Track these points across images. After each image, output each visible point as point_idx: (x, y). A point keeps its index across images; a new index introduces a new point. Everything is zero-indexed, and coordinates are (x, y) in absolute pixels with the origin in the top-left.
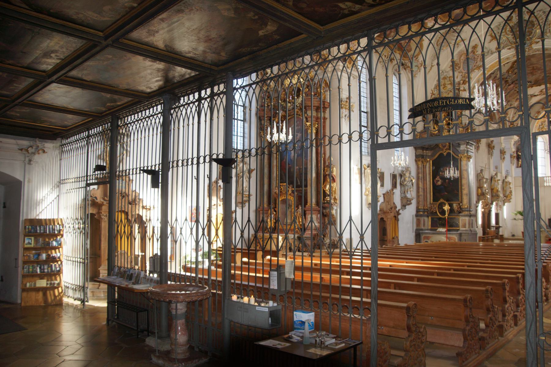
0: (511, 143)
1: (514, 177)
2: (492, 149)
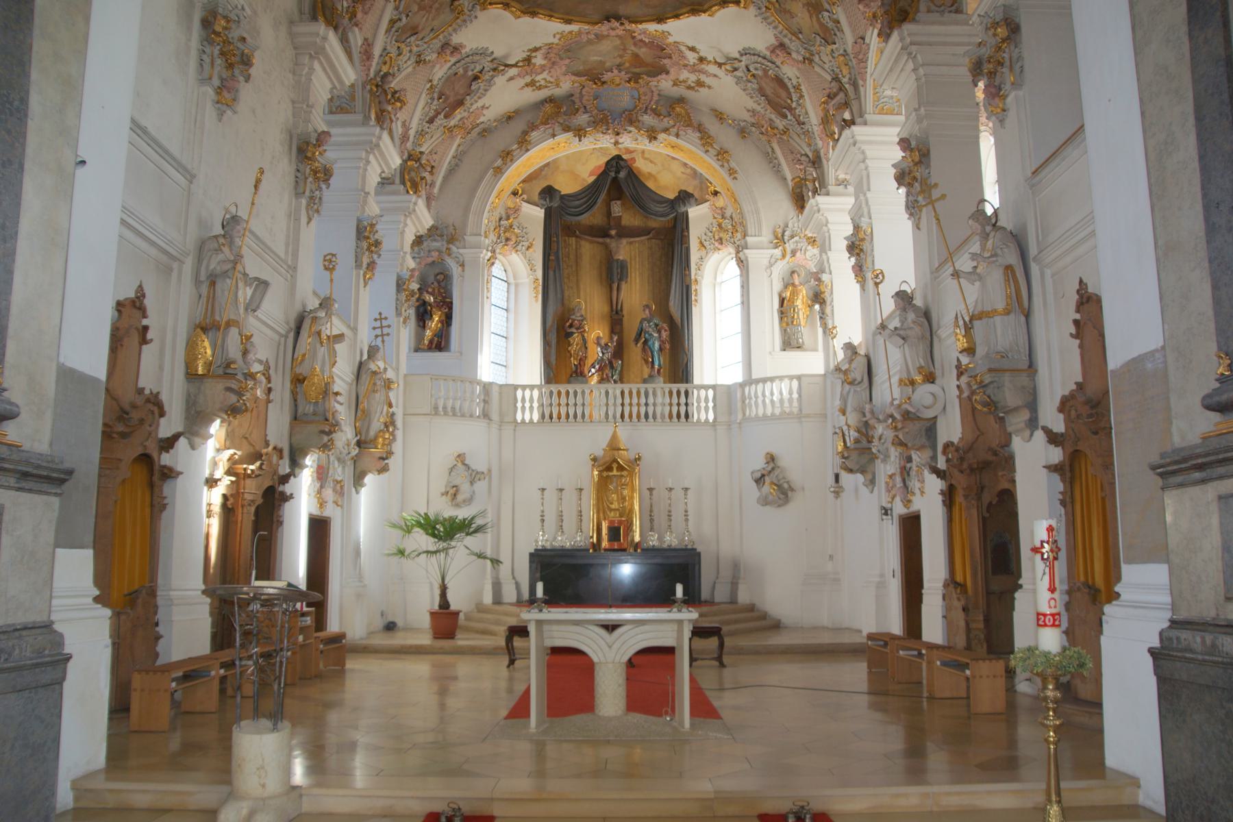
0: (403, 233)
1: (405, 376)
2: (315, 172)
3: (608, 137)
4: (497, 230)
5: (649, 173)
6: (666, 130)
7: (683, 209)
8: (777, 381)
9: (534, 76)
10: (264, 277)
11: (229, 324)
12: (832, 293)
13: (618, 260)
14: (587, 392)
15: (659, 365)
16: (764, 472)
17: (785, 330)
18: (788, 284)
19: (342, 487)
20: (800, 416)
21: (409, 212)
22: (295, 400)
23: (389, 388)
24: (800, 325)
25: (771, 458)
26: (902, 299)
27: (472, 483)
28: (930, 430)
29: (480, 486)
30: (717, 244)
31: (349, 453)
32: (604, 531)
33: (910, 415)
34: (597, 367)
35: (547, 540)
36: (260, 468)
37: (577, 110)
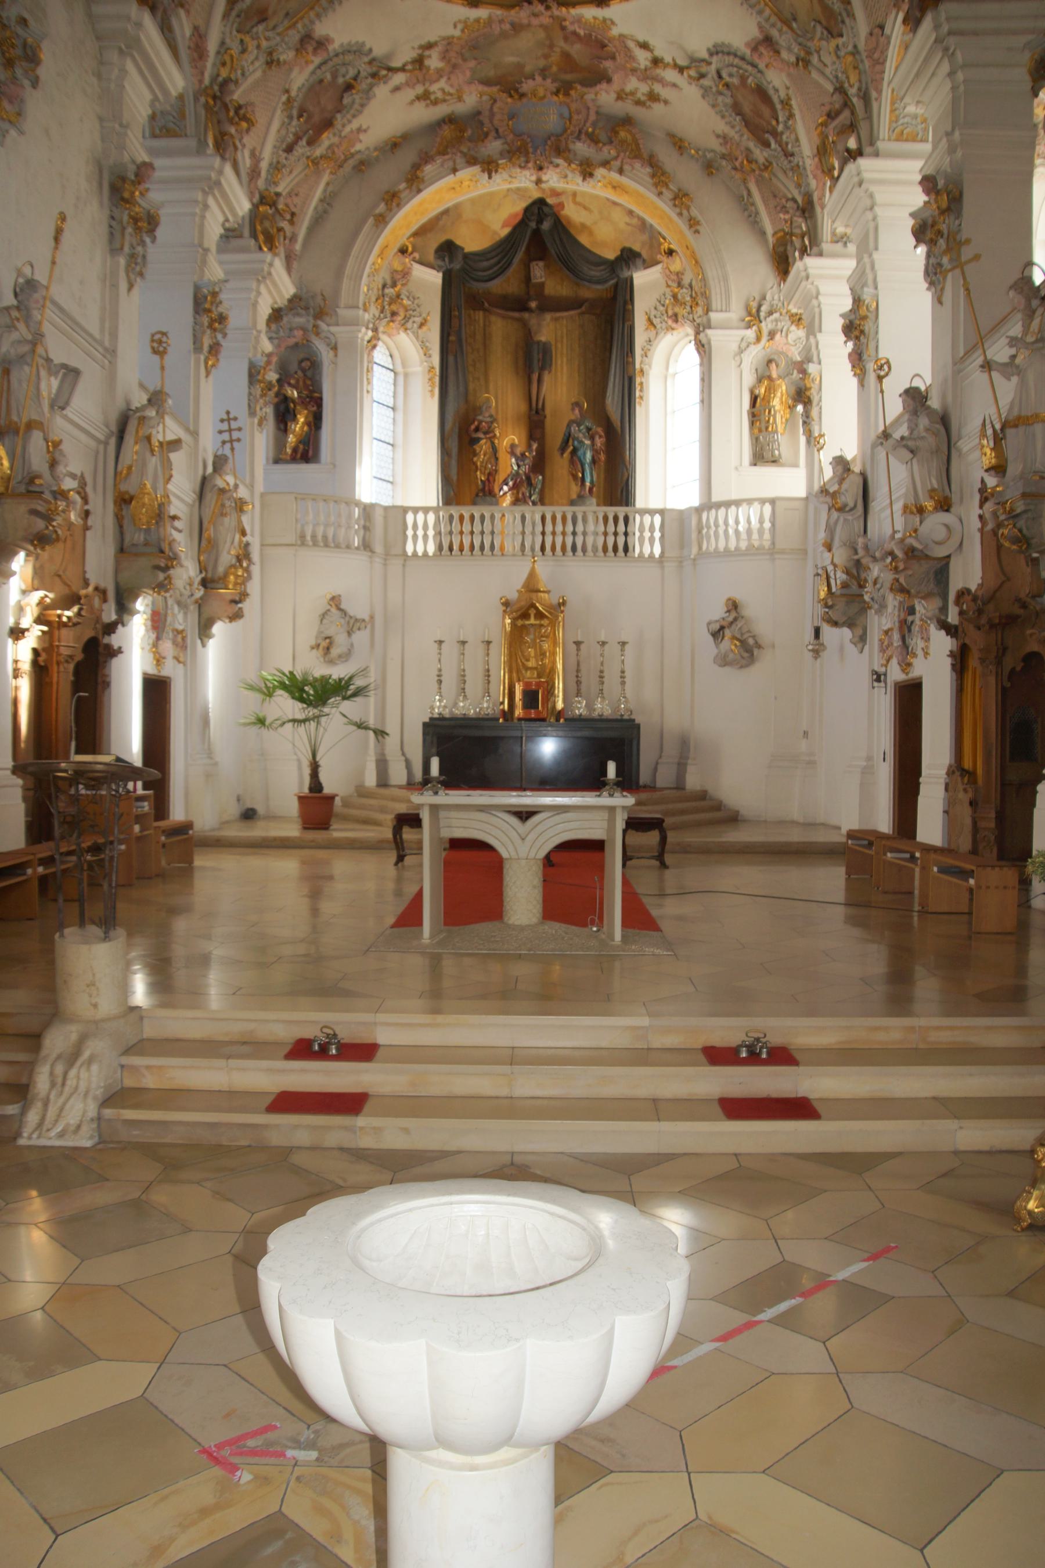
0: (255, 305)
1: (262, 495)
2: (135, 220)
3: (527, 173)
4: (380, 301)
5: (584, 227)
6: (605, 164)
7: (626, 274)
8: (745, 506)
9: (427, 84)
10: (73, 363)
11: (30, 426)
12: (820, 389)
13: (539, 342)
14: (498, 516)
15: (592, 482)
16: (724, 623)
17: (757, 439)
18: (763, 376)
19: (184, 639)
20: (772, 552)
21: (263, 276)
22: (121, 527)
23: (241, 510)
24: (776, 432)
25: (734, 606)
26: (913, 398)
27: (349, 634)
28: (941, 572)
29: (361, 637)
30: (670, 322)
31: (192, 595)
32: (518, 695)
33: (916, 553)
34: (511, 483)
35: (445, 707)
36: (79, 614)
37: (487, 135)
